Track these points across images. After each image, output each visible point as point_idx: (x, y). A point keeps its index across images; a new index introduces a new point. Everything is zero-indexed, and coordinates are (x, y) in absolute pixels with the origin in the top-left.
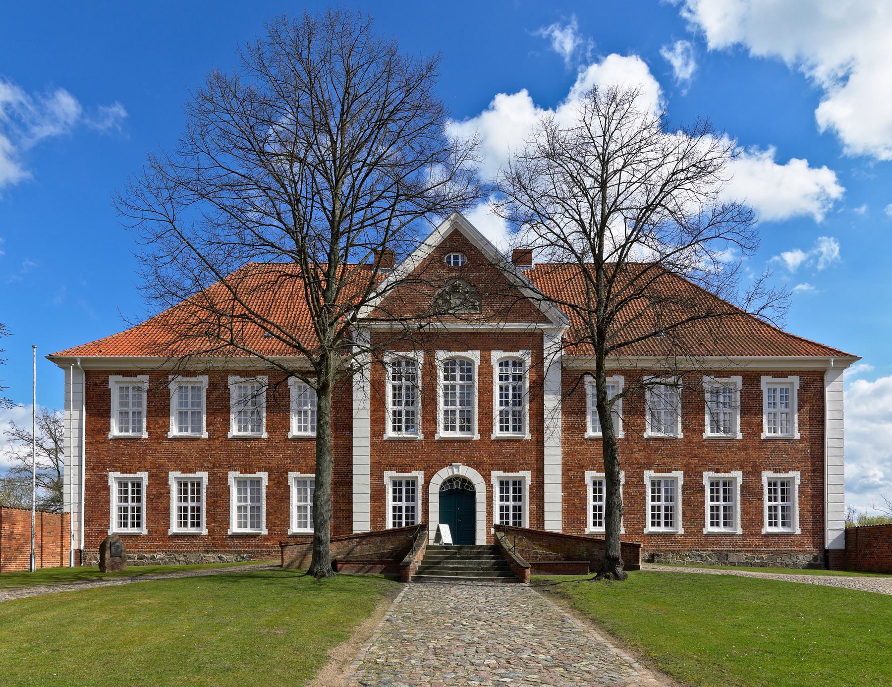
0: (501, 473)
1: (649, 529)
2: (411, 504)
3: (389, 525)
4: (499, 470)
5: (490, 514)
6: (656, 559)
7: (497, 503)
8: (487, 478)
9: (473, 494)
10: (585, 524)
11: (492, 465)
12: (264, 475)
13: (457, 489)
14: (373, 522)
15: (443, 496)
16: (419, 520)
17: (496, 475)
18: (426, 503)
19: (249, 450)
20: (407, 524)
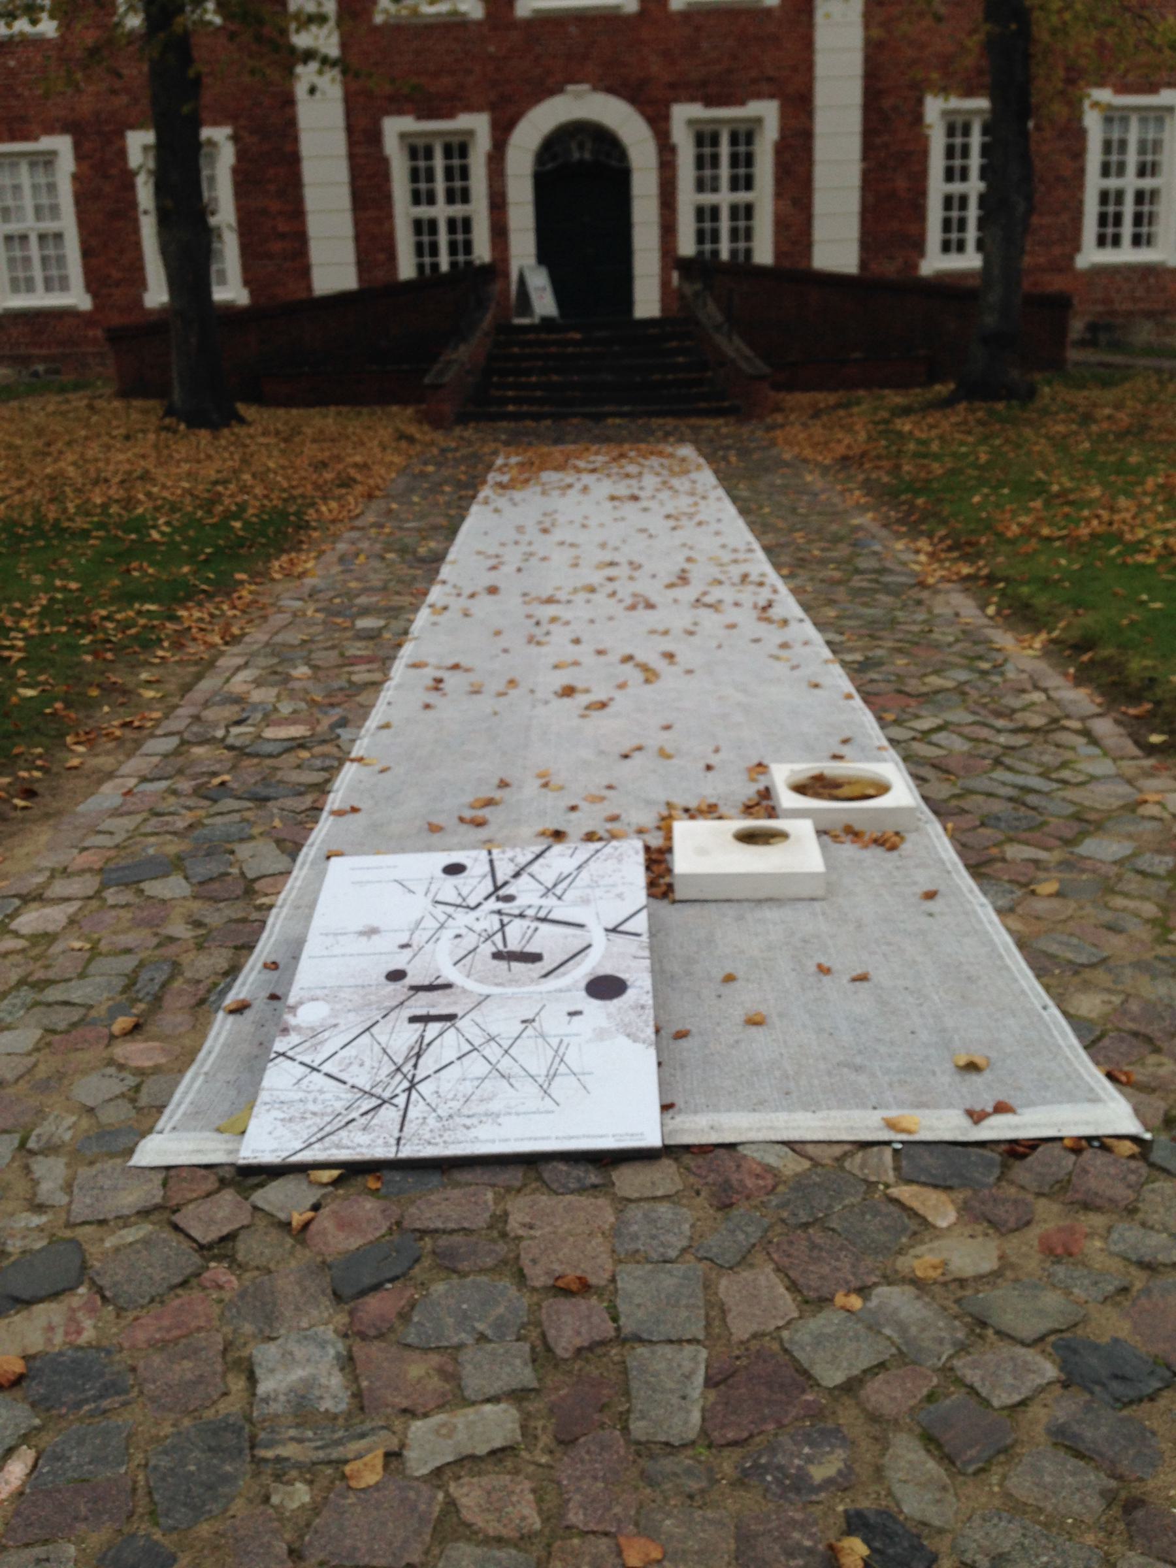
0: (696, 110)
1: (1091, 256)
2: (458, 210)
3: (406, 269)
4: (692, 99)
5: (668, 229)
6: (1103, 337)
7: (687, 199)
8: (659, 124)
9: (622, 176)
10: (918, 246)
11: (672, 86)
12: (62, 144)
13: (581, 162)
14: (363, 264)
15: (542, 182)
16: (482, 251)
17: (684, 114)
18: (498, 204)
19: (12, 73)
20: (453, 265)
